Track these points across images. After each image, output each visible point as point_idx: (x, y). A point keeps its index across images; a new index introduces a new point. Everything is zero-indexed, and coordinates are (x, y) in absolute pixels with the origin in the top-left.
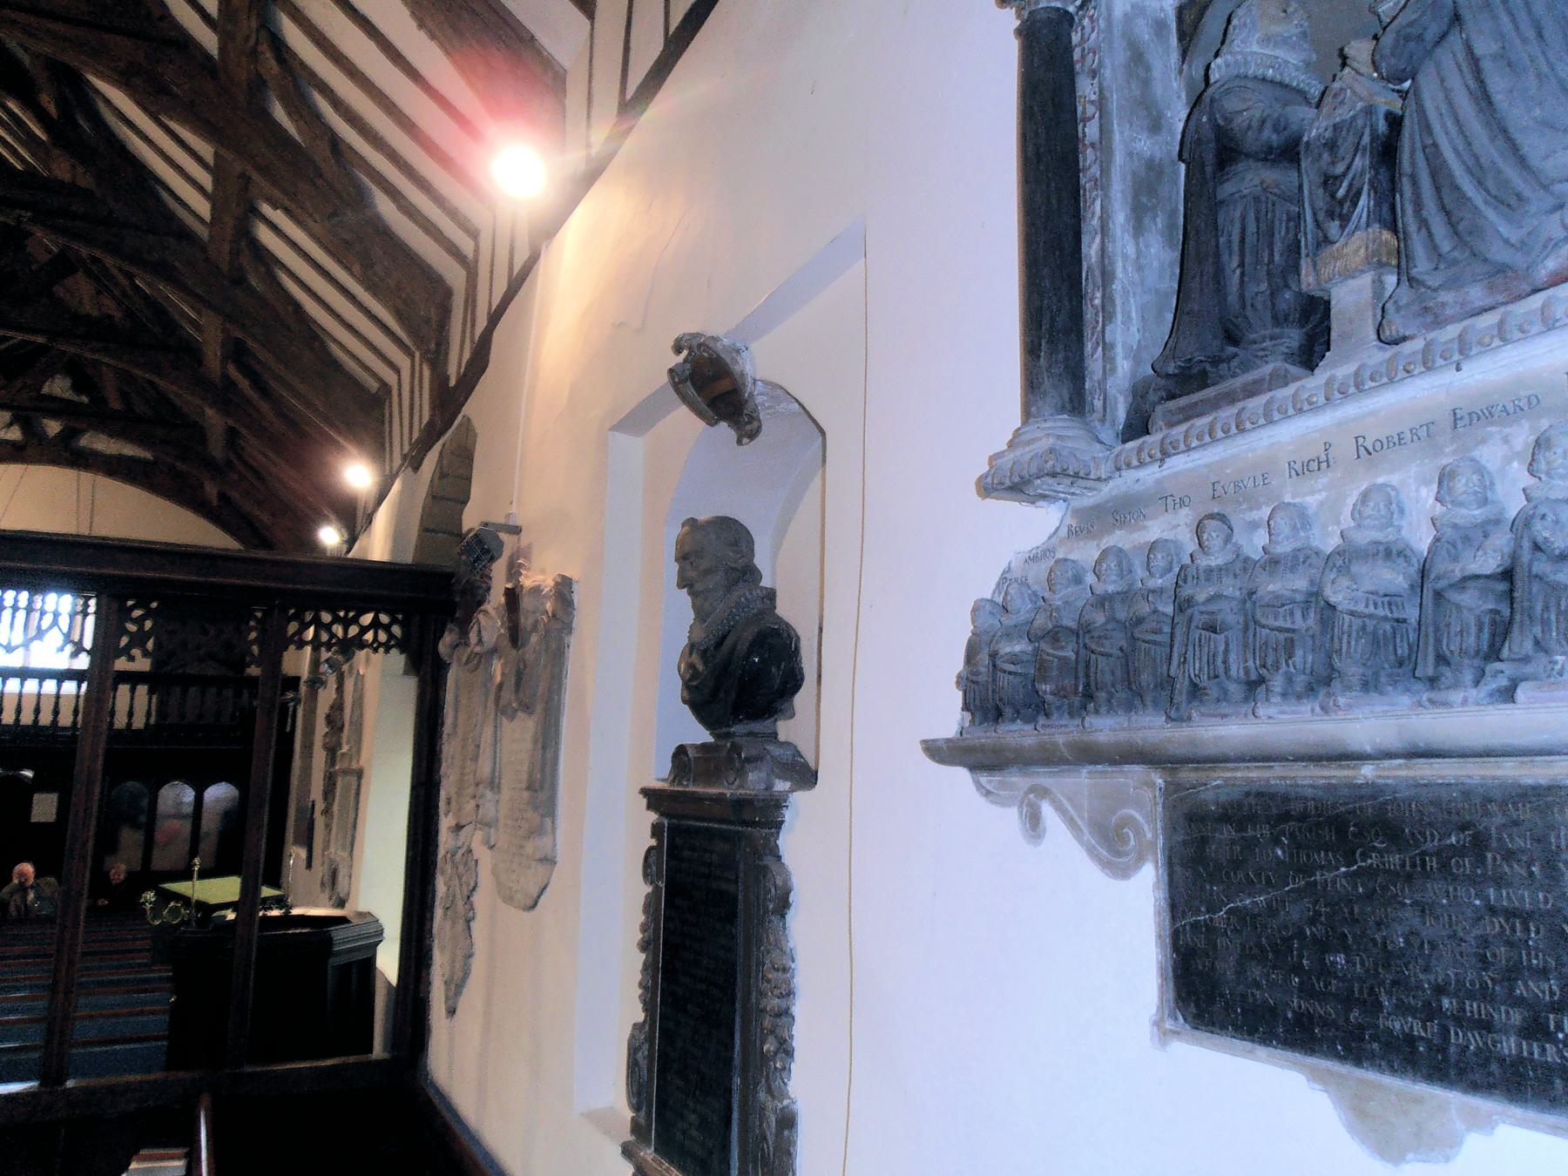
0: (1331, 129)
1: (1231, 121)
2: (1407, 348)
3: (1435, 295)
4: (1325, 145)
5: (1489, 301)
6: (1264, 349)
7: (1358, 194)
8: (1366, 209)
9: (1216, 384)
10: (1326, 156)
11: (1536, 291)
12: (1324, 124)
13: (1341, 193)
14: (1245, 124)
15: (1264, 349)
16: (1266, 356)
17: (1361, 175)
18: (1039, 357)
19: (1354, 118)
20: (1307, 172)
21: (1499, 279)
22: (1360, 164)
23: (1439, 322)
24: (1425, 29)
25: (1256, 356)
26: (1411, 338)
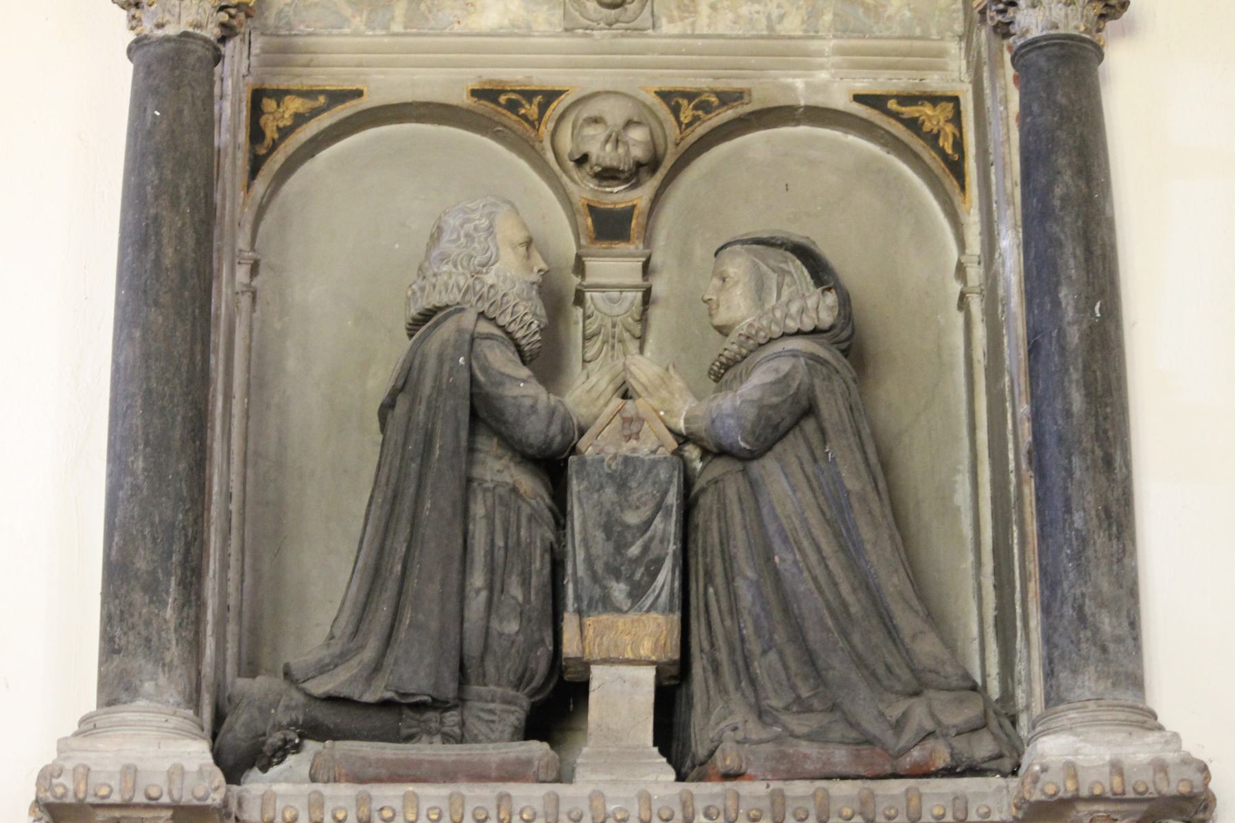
0: (620, 459)
1: (501, 384)
2: (744, 787)
3: (795, 741)
4: (611, 476)
5: (851, 770)
6: (491, 712)
7: (658, 563)
8: (667, 588)
9: (409, 738)
10: (610, 492)
11: (895, 776)
12: (611, 450)
13: (634, 550)
14: (528, 402)
15: (491, 712)
16: (493, 722)
17: (662, 541)
18: (166, 604)
19: (655, 463)
20: (580, 500)
21: (865, 751)
22: (661, 526)
23: (791, 776)
24: (783, 420)
25: (479, 718)
26: (752, 778)
